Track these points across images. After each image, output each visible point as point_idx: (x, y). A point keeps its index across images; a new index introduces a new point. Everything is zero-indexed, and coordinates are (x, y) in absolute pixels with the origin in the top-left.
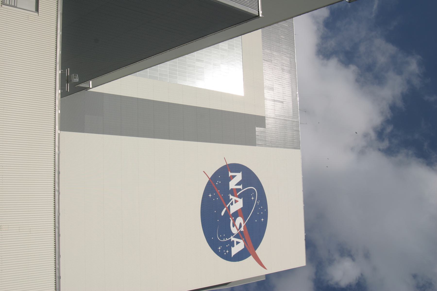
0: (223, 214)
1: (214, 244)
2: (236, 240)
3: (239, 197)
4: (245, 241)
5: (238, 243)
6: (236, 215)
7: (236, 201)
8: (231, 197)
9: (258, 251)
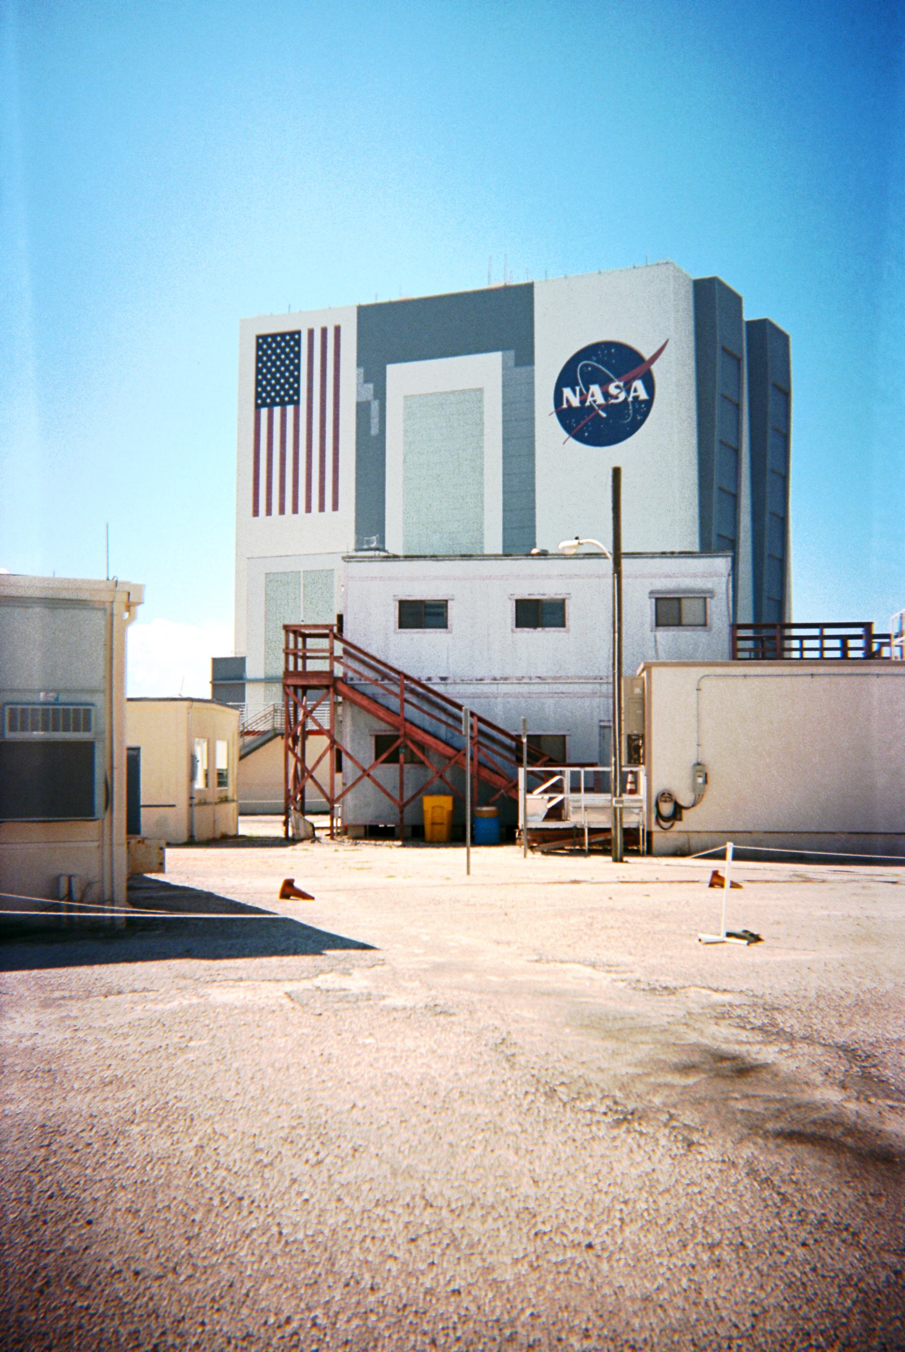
0: (604, 415)
1: (635, 426)
2: (632, 394)
3: (588, 390)
4: (634, 379)
5: (635, 391)
6: (606, 395)
7: (593, 396)
8: (588, 404)
9: (647, 356)
